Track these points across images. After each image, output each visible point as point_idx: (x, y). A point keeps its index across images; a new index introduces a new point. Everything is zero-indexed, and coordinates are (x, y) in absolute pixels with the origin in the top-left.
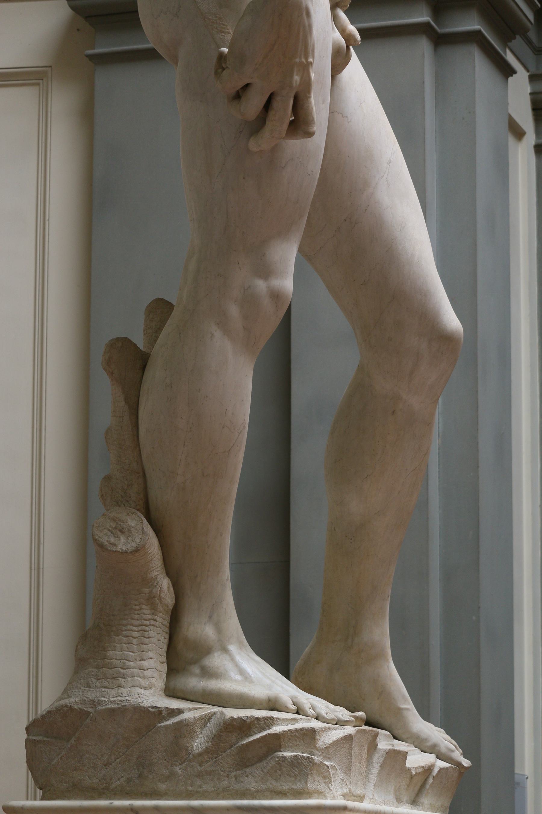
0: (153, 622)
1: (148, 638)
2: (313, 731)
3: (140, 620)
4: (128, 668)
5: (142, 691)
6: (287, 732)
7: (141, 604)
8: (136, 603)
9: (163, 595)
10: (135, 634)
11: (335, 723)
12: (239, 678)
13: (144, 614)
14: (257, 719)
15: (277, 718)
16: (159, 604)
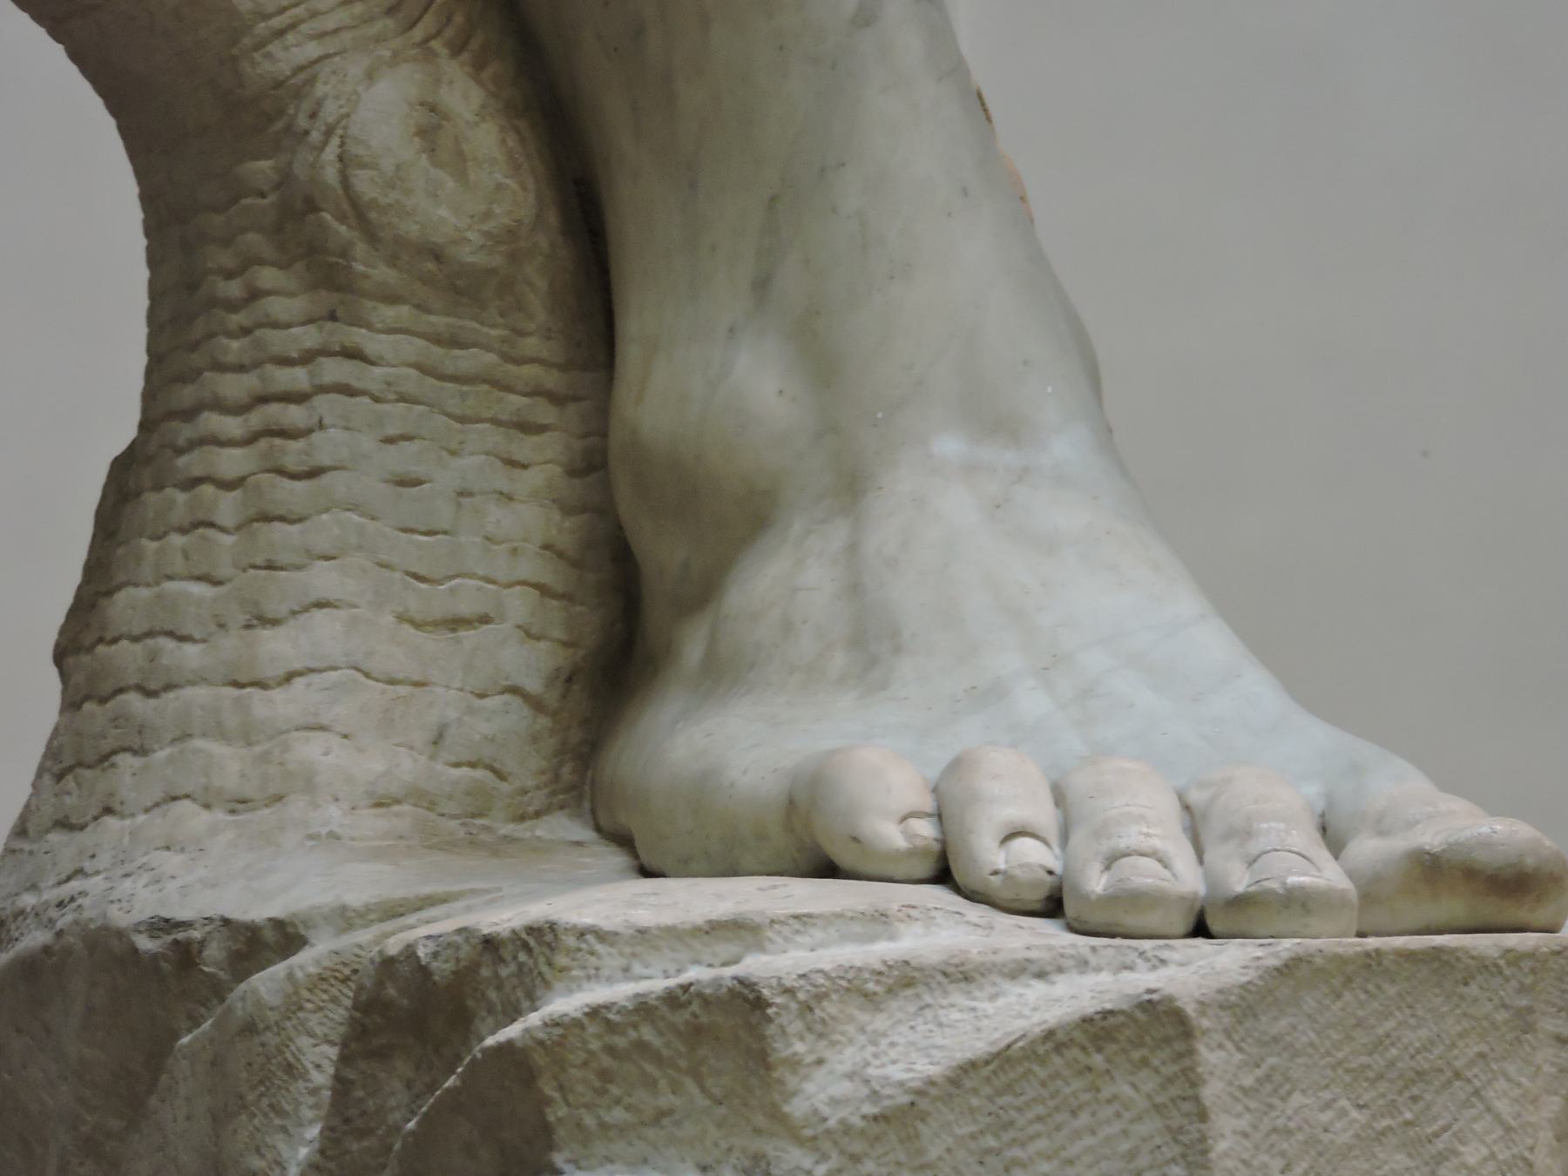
0: (335, 370)
1: (314, 473)
2: (748, 1002)
3: (257, 364)
4: (169, 687)
5: (193, 819)
6: (577, 1024)
7: (250, 262)
8: (226, 259)
9: (365, 184)
10: (231, 462)
11: (1183, 923)
12: (839, 660)
13: (276, 325)
14: (490, 944)
15: (582, 933)
16: (360, 249)
